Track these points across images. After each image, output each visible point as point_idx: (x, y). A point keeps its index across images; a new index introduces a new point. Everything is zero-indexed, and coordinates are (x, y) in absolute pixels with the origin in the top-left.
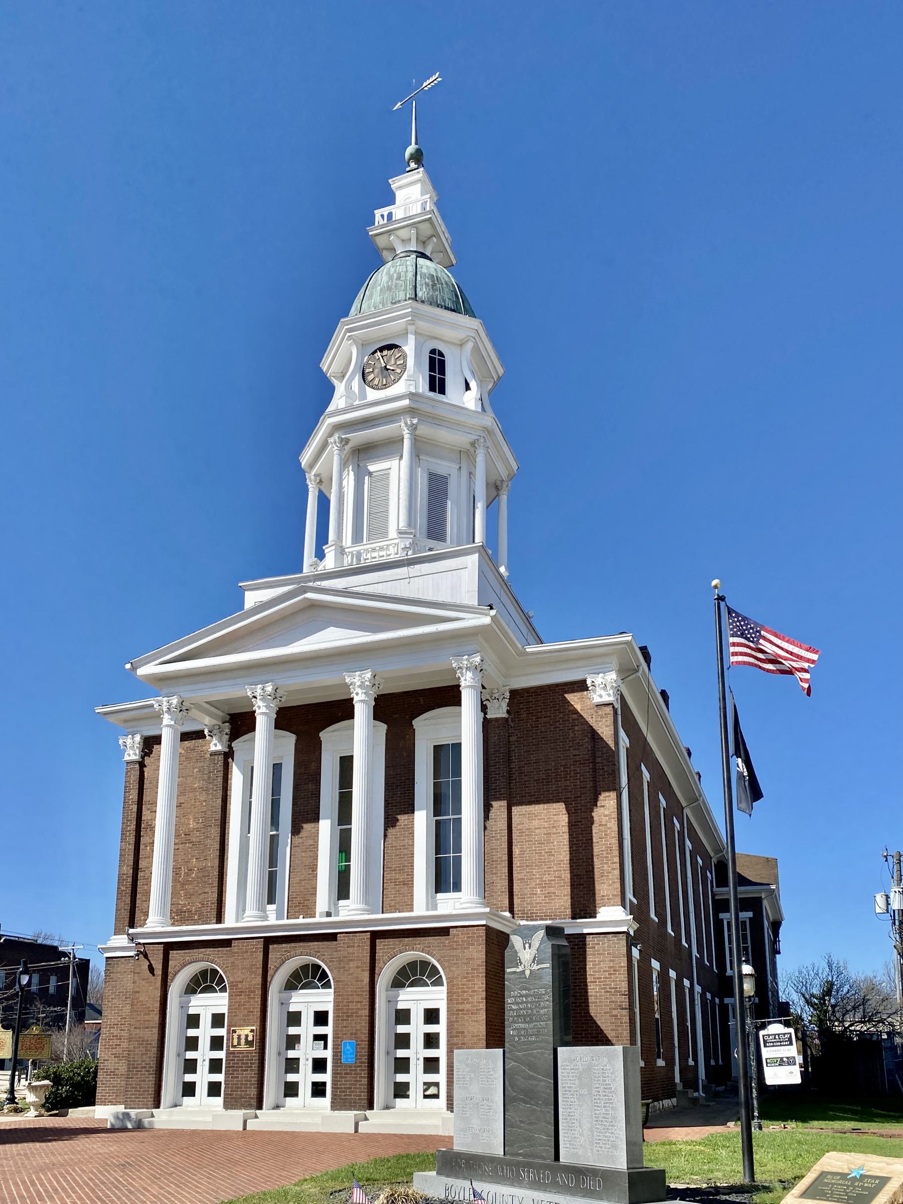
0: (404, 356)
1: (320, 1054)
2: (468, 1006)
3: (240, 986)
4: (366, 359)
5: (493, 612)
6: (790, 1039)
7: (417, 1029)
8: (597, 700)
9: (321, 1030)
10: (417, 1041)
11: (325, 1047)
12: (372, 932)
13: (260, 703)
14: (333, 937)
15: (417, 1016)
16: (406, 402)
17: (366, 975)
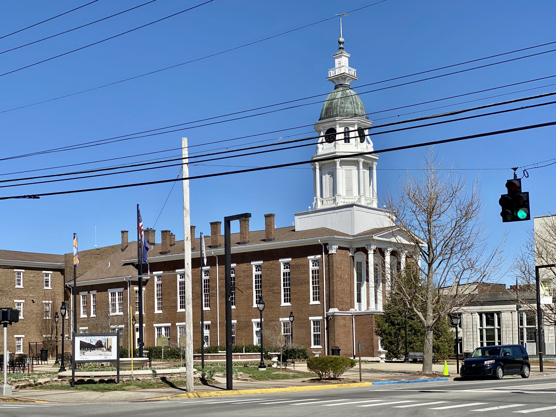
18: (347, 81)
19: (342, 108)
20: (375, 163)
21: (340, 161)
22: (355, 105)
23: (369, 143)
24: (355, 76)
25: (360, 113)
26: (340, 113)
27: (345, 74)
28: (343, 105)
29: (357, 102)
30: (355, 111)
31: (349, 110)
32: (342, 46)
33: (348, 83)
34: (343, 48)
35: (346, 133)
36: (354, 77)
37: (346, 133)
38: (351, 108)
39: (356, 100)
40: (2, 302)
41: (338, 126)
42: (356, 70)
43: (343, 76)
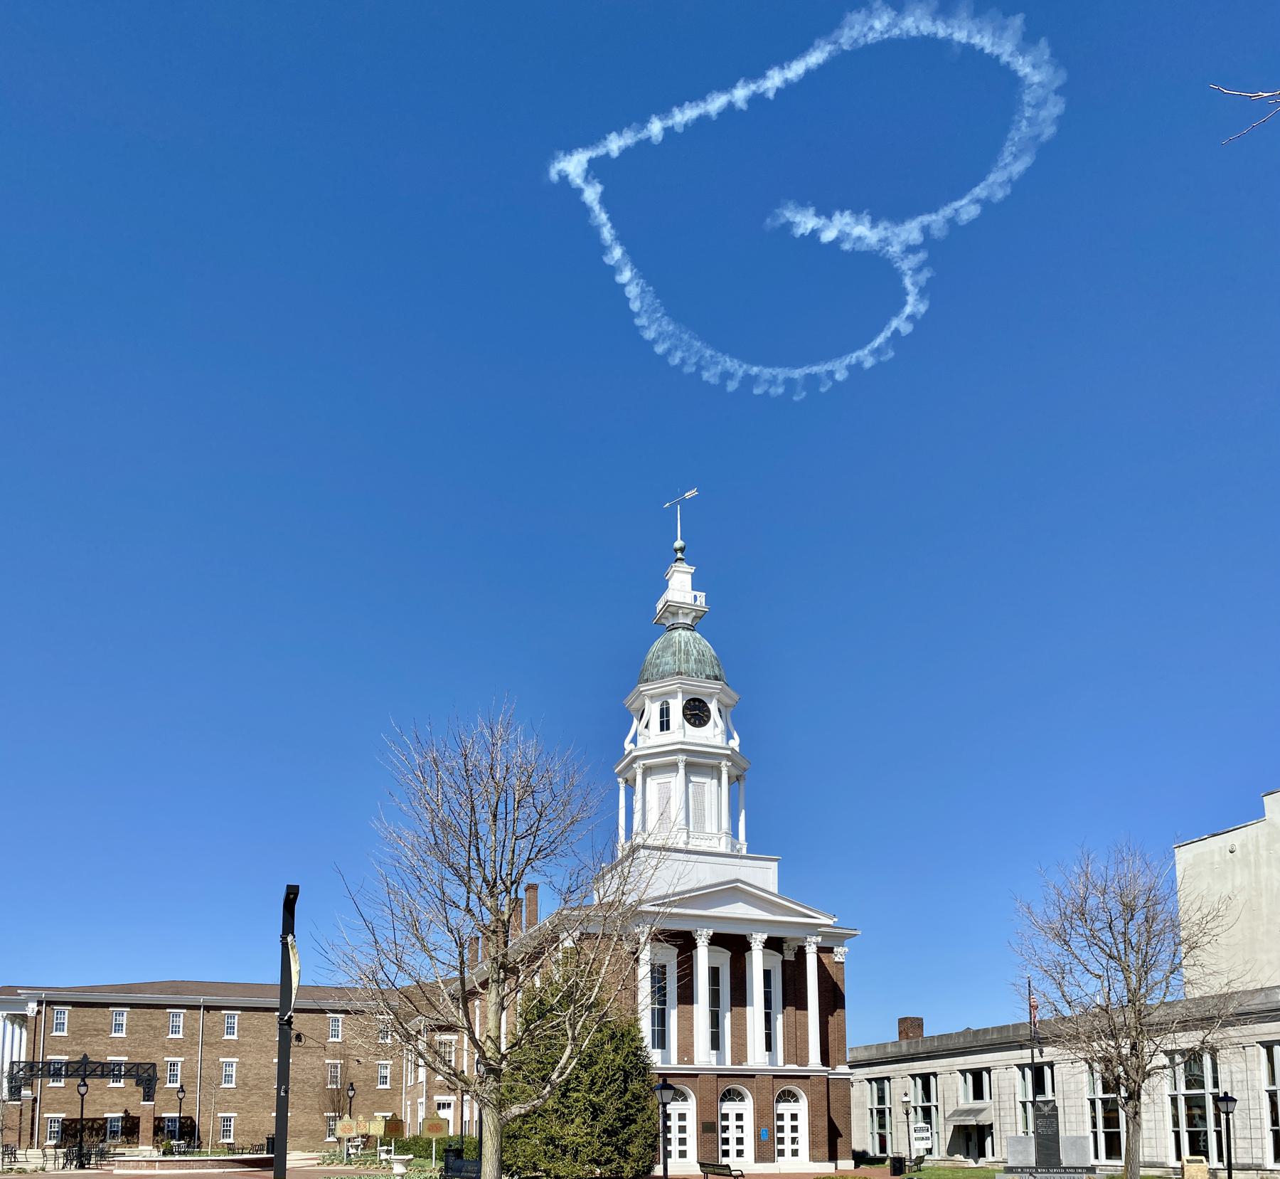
0: (709, 711)
1: (740, 1135)
2: (820, 1113)
3: (705, 1099)
4: (684, 702)
5: (836, 920)
6: (928, 1130)
7: (787, 1123)
8: (837, 959)
9: (739, 1123)
10: (787, 1129)
11: (742, 1132)
12: (773, 1075)
13: (703, 939)
14: (753, 1076)
15: (787, 1117)
16: (729, 752)
17: (771, 1096)
18: (680, 616)
19: (657, 665)
20: (723, 763)
21: (642, 766)
22: (683, 656)
23: (716, 725)
24: (704, 605)
25: (692, 669)
26: (652, 676)
27: (669, 603)
28: (658, 661)
29: (688, 650)
30: (679, 668)
31: (667, 667)
32: (679, 555)
33: (687, 620)
34: (683, 560)
35: (665, 712)
36: (702, 607)
37: (665, 712)
38: (673, 663)
39: (686, 646)
40: (305, 1063)
41: (647, 702)
42: (705, 594)
43: (673, 609)
